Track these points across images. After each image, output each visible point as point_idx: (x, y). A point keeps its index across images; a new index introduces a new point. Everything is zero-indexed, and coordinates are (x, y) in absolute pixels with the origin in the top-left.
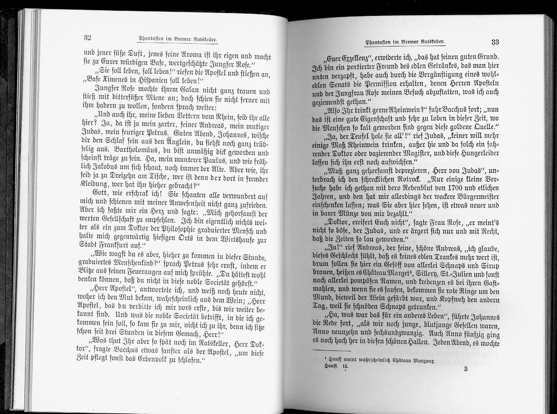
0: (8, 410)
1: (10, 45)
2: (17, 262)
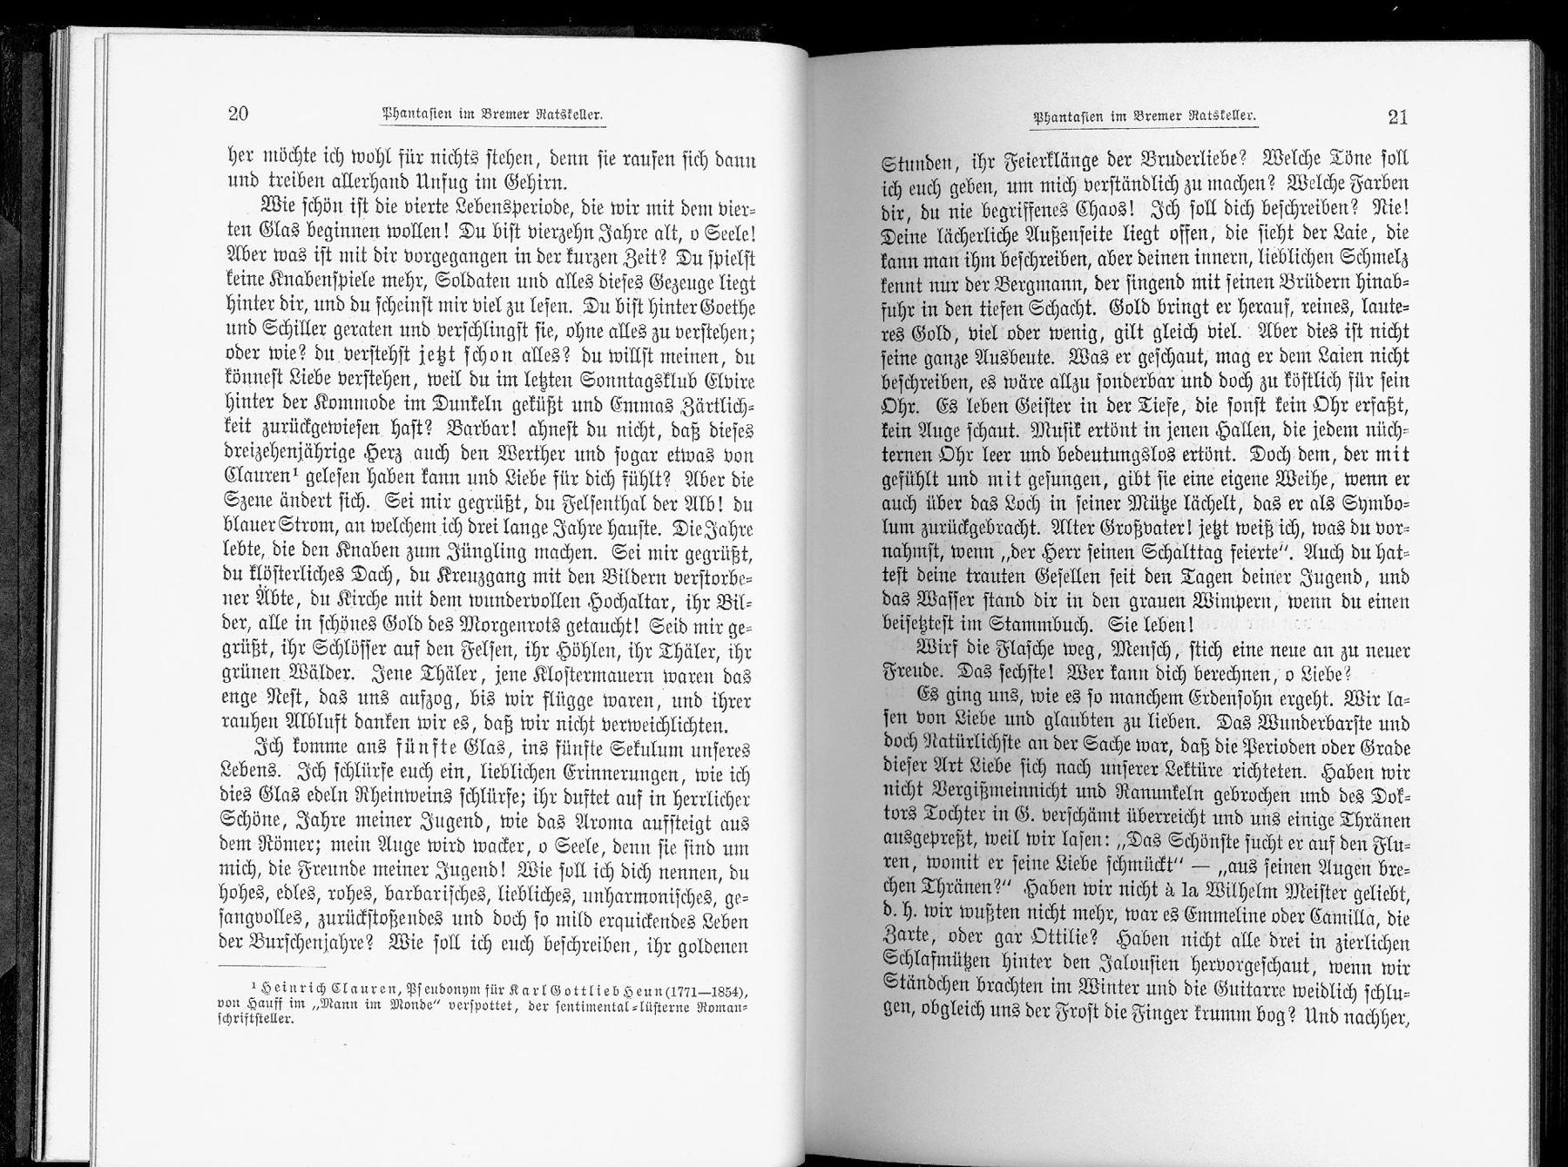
1: (29, 129)
2: (53, 744)
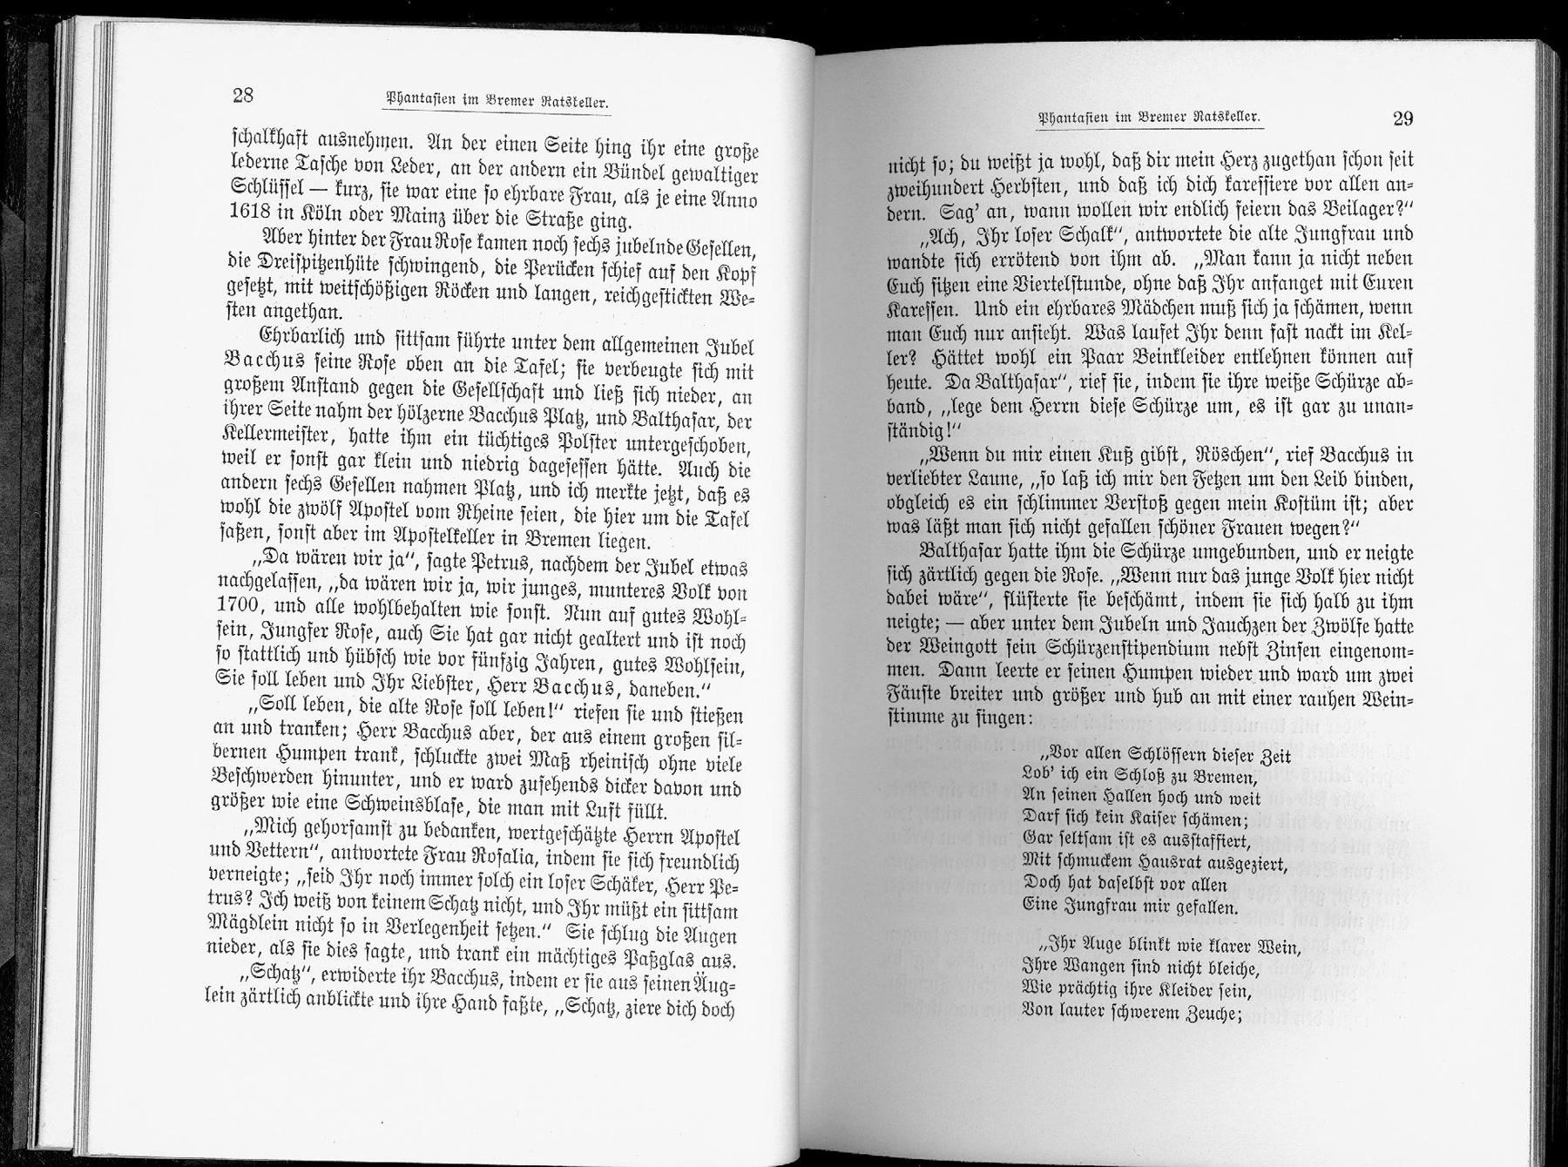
0: (25, 1151)
1: (33, 119)
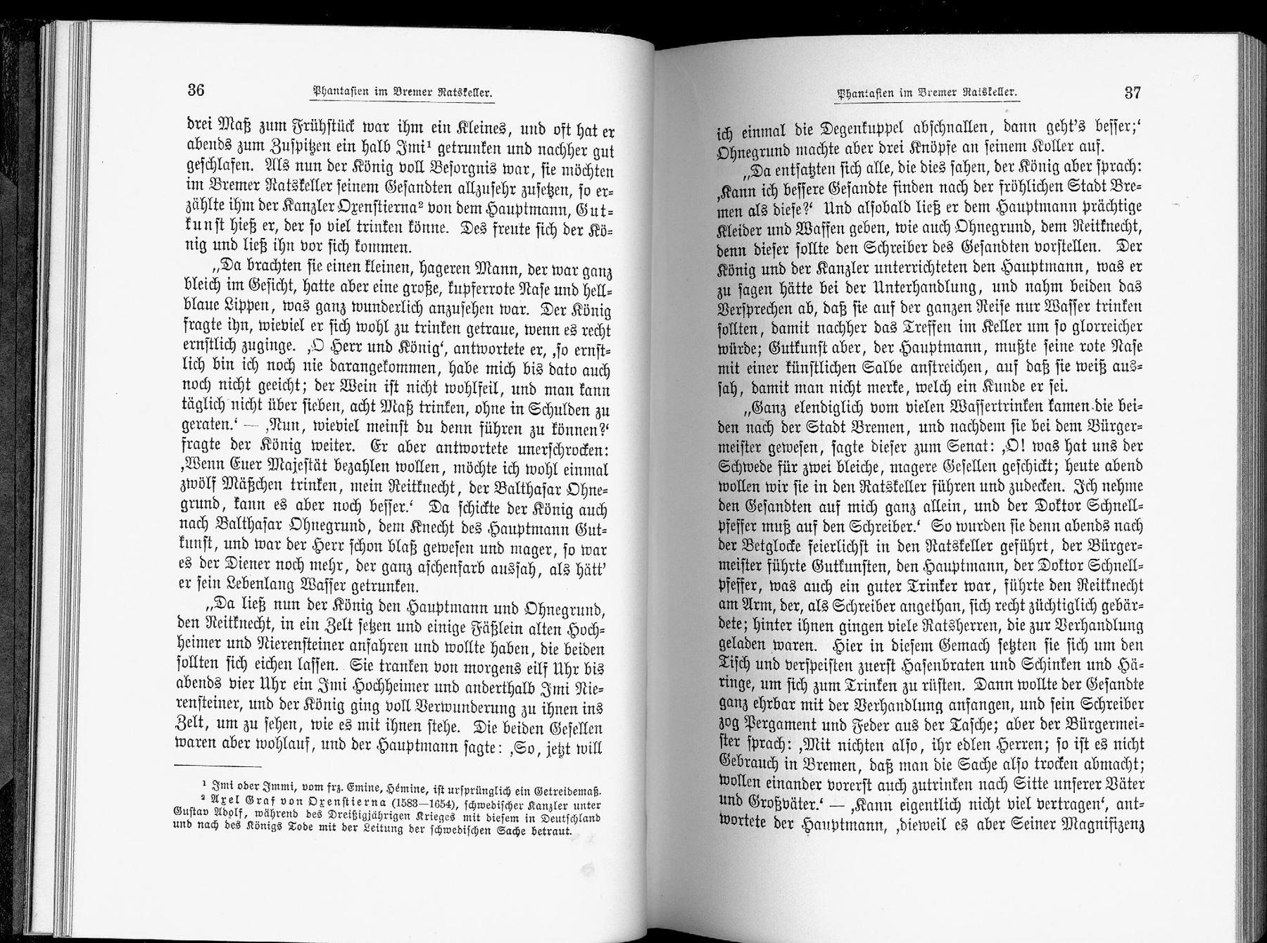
1: (23, 103)
2: (40, 598)
